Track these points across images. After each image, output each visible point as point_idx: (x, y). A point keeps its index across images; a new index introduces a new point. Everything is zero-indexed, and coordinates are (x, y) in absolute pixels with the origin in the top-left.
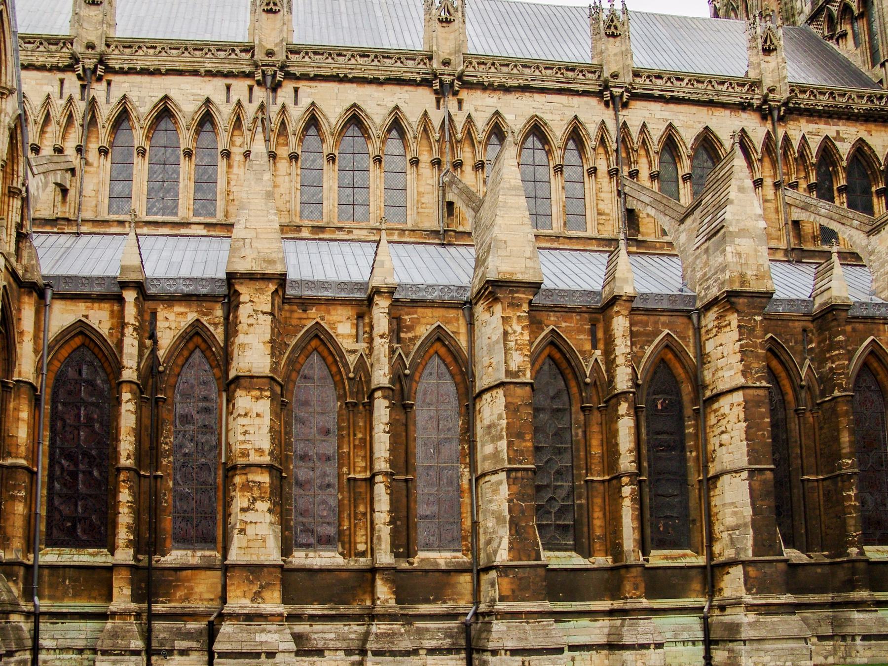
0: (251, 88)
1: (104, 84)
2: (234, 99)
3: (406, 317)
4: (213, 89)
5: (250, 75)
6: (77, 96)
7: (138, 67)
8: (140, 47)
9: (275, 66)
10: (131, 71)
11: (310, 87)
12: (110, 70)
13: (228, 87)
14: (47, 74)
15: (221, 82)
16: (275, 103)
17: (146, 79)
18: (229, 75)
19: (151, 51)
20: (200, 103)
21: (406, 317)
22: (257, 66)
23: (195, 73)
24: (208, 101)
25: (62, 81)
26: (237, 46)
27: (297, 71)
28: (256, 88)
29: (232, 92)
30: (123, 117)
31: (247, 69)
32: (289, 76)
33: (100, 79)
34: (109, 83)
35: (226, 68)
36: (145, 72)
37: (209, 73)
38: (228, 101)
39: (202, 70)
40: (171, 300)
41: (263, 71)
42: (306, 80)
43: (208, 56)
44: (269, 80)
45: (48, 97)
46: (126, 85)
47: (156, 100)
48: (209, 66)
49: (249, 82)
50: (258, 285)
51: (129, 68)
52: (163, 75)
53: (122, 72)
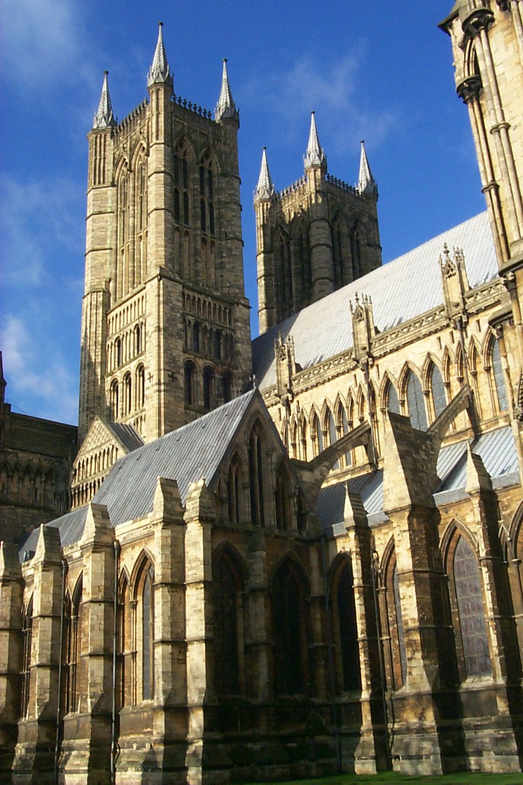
0: (452, 333)
1: (375, 368)
2: (443, 347)
3: (504, 500)
4: (430, 345)
5: (448, 326)
6: (364, 382)
7: (388, 350)
8: (387, 337)
9: (459, 313)
10: (385, 354)
11: (486, 315)
12: (374, 359)
13: (439, 339)
14: (347, 375)
15: (434, 338)
16: (467, 337)
17: (395, 354)
18: (436, 331)
19: (393, 336)
20: (425, 358)
21: (504, 500)
22: (450, 319)
23: (418, 339)
24: (429, 354)
25: (355, 376)
26: (436, 310)
27: (473, 310)
28: (454, 332)
29: (442, 341)
30: (388, 385)
31: (445, 323)
32: (469, 315)
33: (372, 366)
34: (377, 366)
35: (434, 327)
36: (391, 351)
37: (425, 336)
38: (441, 348)
39: (421, 336)
40: (379, 526)
41: (454, 320)
42: (482, 312)
43: (423, 324)
44: (458, 324)
45: (350, 390)
46: (386, 363)
47: (402, 366)
48: (424, 332)
49: (449, 330)
50: (400, 514)
51: (384, 353)
52: (403, 348)
53: (381, 357)
